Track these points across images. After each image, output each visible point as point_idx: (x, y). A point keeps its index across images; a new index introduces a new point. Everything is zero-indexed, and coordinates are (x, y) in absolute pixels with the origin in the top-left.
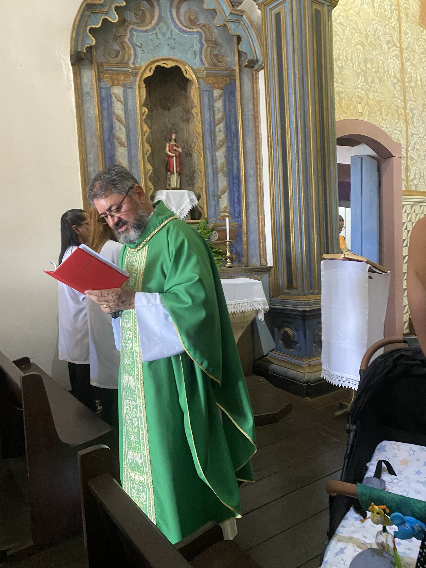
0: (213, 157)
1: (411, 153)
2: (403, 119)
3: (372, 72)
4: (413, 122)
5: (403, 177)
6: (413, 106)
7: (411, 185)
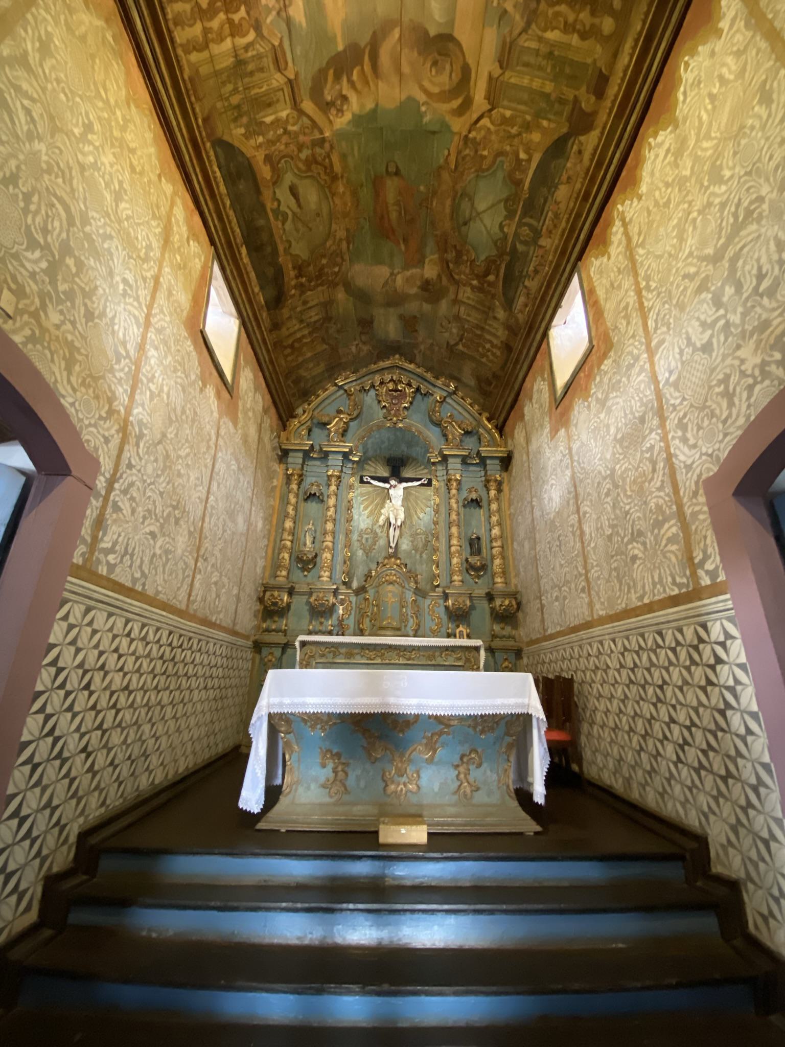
1: (119, 496)
2: (119, 424)
3: (74, 282)
4: (138, 445)
5: (86, 531)
6: (145, 421)
7: (99, 562)
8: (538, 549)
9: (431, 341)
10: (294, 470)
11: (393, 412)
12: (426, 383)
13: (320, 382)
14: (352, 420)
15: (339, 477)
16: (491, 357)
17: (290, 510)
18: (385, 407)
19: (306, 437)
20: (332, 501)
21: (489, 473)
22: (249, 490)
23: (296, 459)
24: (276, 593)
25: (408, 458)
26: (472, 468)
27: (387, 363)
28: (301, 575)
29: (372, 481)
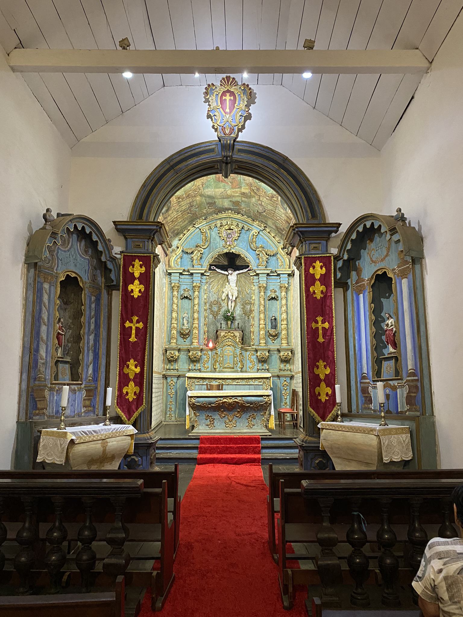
0: (88, 339)
11: (228, 243)
19: (179, 263)
20: (196, 302)
23: (175, 278)
24: (172, 352)
26: (273, 277)
27: (224, 215)
28: (183, 340)
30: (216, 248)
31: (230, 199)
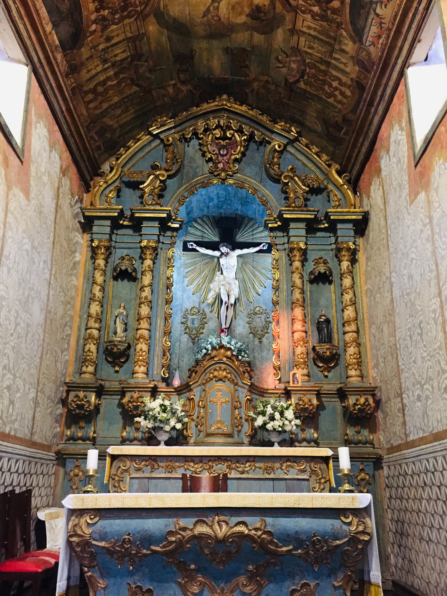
8: (397, 338)
9: (266, 78)
10: (100, 241)
11: (221, 166)
12: (261, 129)
13: (131, 131)
14: (169, 177)
15: (155, 249)
16: (340, 97)
17: (97, 290)
18: (210, 159)
19: (113, 201)
20: (147, 280)
21: (340, 239)
22: (46, 270)
23: (102, 229)
24: (81, 394)
25: (243, 218)
26: (319, 234)
28: (112, 370)
29: (198, 248)
30: (195, 176)
31: (226, 43)
